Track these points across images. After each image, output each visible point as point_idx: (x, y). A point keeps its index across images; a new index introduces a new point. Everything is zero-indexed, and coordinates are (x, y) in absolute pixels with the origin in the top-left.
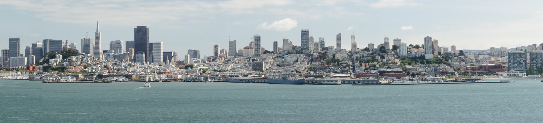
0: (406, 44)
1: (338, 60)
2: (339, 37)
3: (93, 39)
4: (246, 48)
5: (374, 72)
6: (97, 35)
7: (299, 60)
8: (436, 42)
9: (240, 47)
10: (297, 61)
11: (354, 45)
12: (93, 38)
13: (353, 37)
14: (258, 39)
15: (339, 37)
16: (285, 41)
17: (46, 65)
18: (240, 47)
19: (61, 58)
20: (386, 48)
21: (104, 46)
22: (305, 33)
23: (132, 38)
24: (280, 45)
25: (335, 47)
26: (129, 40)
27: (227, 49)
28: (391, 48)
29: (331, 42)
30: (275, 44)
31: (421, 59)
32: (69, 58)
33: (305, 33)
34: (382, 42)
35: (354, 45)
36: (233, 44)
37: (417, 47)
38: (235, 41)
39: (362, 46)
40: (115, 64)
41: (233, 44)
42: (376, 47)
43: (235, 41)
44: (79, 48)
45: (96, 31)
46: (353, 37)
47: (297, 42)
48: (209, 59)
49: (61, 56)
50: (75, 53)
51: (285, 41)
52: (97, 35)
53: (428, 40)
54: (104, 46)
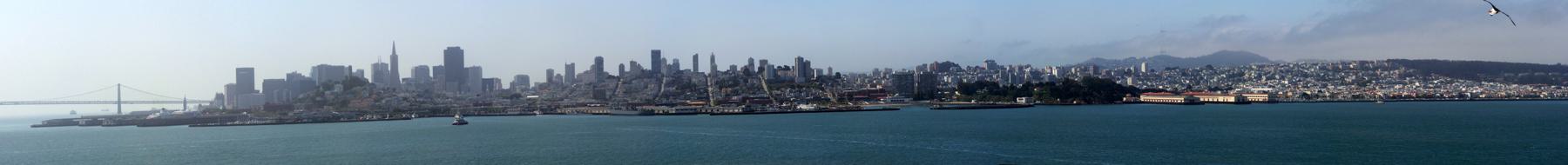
0: (773, 66)
1: (695, 85)
2: (696, 58)
3: (387, 65)
4: (586, 72)
5: (735, 98)
6: (394, 58)
8: (808, 63)
9: (578, 70)
10: (647, 87)
11: (714, 67)
12: (387, 61)
14: (599, 61)
15: (696, 58)
16: (633, 64)
17: (318, 99)
18: (578, 70)
20: (751, 70)
21: (405, 72)
22: (656, 55)
23: (440, 62)
24: (627, 69)
25: (691, 68)
26: (437, 65)
27: (563, 73)
28: (756, 70)
29: (686, 65)
30: (622, 67)
31: (791, 83)
32: (354, 89)
33: (656, 55)
34: (747, 63)
35: (714, 67)
36: (570, 68)
37: (787, 68)
38: (573, 65)
39: (723, 67)
41: (570, 68)
42: (739, 69)
43: (573, 65)
44: (368, 76)
47: (647, 65)
48: (541, 87)
50: (363, 82)
51: (633, 64)
52: (394, 58)
53: (800, 60)
54: (405, 72)
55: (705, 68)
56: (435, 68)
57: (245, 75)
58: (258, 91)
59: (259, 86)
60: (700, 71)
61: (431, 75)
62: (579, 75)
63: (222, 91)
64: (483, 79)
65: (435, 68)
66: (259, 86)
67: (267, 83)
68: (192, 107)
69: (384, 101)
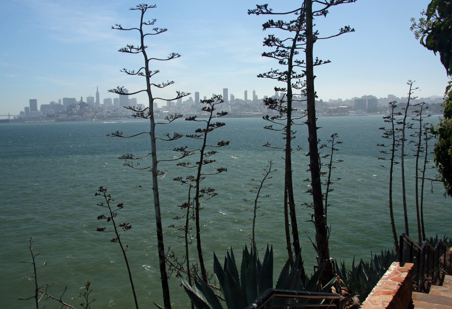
2: (246, 92)
3: (94, 97)
4: (187, 101)
6: (98, 94)
7: (223, 106)
10: (222, 107)
12: (95, 96)
13: (254, 92)
15: (246, 92)
17: (70, 112)
19: (79, 108)
21: (102, 102)
25: (244, 99)
29: (240, 96)
32: (84, 107)
35: (255, 97)
40: (113, 110)
45: (96, 92)
46: (254, 92)
49: (79, 106)
52: (98, 94)
54: (102, 102)
55: (250, 97)
56: (114, 99)
57: (33, 102)
58: (38, 110)
59: (39, 108)
60: (248, 99)
61: (113, 103)
62: (184, 102)
63: (23, 110)
64: (138, 104)
65: (114, 99)
66: (39, 108)
67: (43, 107)
68: (12, 118)
69: (99, 113)
